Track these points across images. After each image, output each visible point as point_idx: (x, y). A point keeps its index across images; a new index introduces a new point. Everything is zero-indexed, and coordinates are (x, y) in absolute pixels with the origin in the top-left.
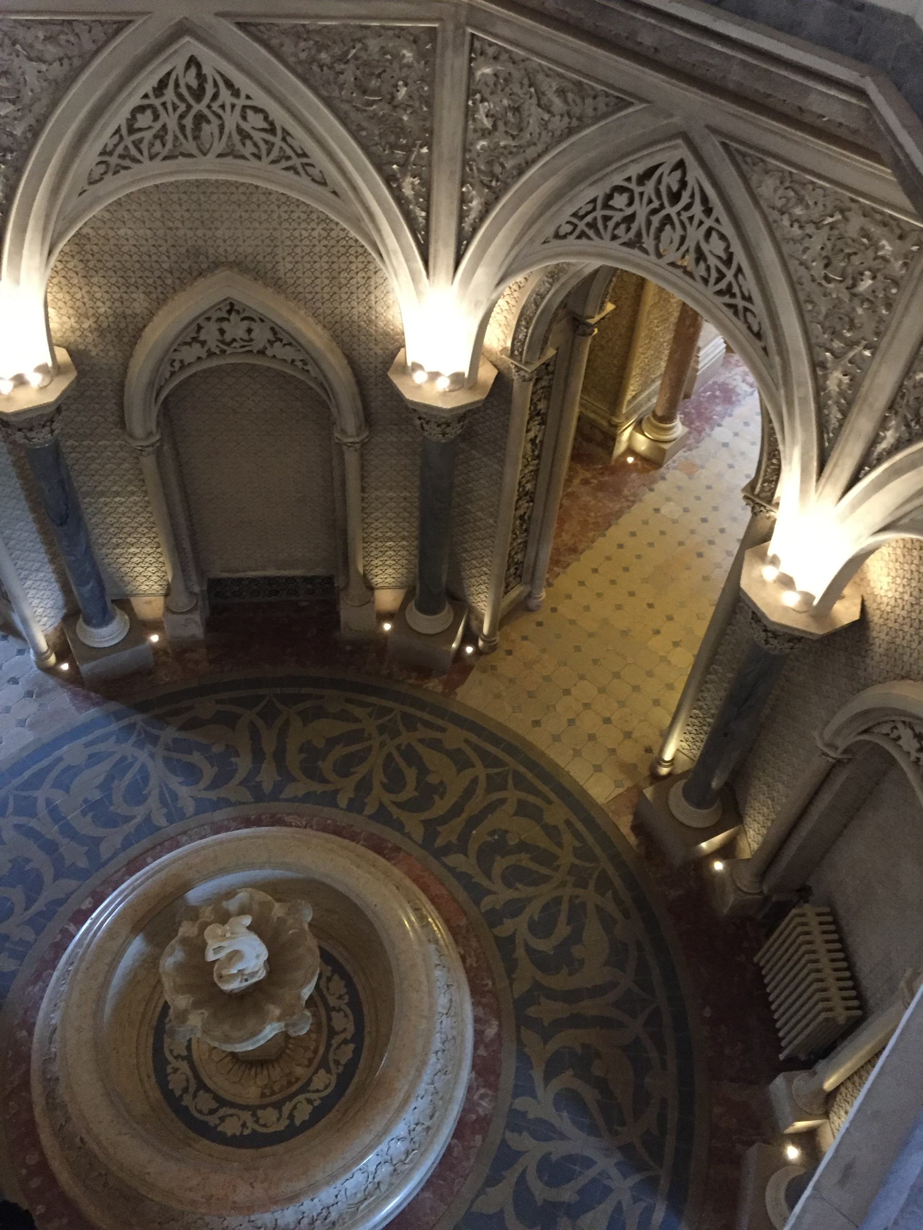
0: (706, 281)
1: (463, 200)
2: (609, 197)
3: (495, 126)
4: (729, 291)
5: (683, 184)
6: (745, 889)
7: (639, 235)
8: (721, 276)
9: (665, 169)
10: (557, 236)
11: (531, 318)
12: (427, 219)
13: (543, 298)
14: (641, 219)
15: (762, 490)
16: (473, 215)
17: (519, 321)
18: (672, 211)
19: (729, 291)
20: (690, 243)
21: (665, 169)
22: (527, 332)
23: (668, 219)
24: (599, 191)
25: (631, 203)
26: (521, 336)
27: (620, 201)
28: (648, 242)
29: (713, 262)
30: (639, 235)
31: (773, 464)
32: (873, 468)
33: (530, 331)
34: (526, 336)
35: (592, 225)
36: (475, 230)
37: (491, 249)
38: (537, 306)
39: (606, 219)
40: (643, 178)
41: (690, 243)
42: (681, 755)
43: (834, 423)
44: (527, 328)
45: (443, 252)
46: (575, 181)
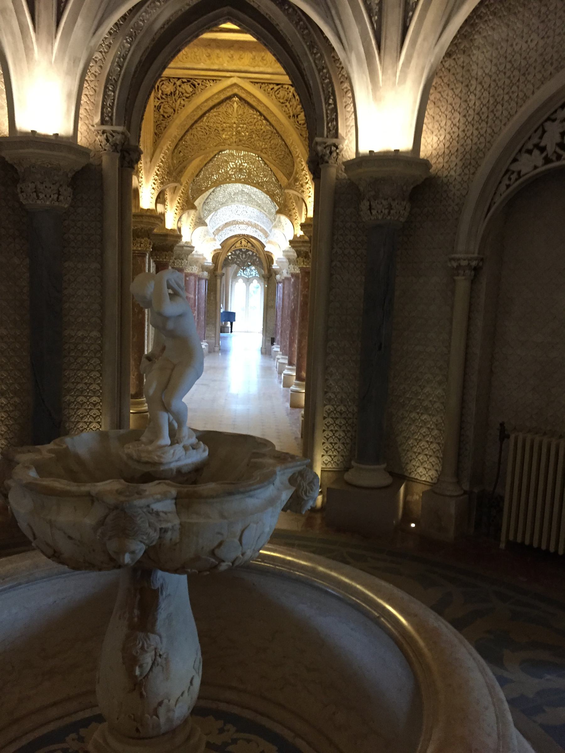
6: (456, 494)
11: (116, 82)
13: (124, 59)
15: (329, 130)
17: (106, 87)
22: (114, 96)
26: (109, 103)
31: (330, 104)
32: (414, 11)
33: (117, 92)
34: (114, 100)
37: (79, 21)
38: (121, 67)
42: (326, 474)
43: (376, 9)
44: (114, 92)
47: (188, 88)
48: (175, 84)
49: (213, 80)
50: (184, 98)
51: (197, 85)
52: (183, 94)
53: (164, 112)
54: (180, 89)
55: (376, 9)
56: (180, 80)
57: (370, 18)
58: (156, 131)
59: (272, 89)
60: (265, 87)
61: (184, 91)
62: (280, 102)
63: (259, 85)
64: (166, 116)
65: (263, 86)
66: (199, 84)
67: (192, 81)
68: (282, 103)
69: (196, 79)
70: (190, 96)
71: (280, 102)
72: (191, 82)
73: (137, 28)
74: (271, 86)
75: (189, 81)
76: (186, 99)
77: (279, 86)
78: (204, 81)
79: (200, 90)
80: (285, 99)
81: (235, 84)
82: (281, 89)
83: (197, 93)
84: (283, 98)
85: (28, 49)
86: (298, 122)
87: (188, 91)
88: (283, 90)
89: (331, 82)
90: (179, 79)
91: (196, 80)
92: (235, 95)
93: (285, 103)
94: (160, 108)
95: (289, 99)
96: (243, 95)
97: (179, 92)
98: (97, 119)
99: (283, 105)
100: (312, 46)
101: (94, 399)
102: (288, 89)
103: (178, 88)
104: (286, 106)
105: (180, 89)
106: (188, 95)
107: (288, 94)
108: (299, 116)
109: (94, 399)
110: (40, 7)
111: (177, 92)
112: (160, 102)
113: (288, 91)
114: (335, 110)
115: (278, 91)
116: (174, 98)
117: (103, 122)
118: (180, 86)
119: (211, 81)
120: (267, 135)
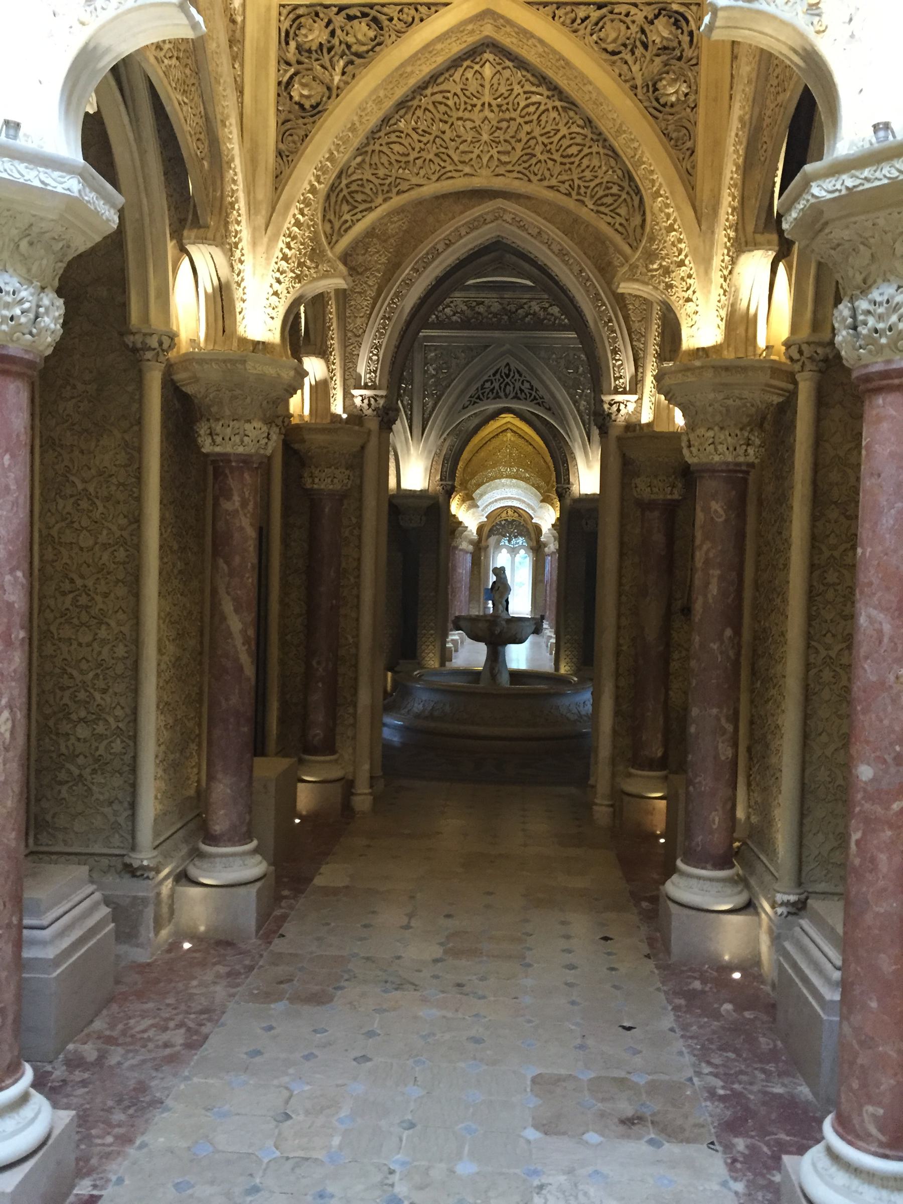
0: (526, 399)
1: (424, 405)
2: (484, 384)
3: (437, 373)
4: (535, 399)
5: (510, 370)
7: (497, 393)
8: (531, 394)
9: (503, 368)
10: (464, 408)
12: (411, 414)
14: (497, 387)
16: (428, 412)
18: (507, 380)
19: (535, 399)
20: (517, 388)
21: (503, 368)
23: (507, 384)
24: (479, 385)
25: (492, 383)
27: (488, 385)
28: (502, 394)
29: (527, 391)
30: (497, 393)
35: (478, 398)
36: (430, 415)
39: (483, 394)
40: (494, 375)
41: (517, 388)
45: (417, 430)
46: (468, 385)
55: (587, 421)
57: (584, 426)
73: (460, 431)
85: (408, 449)
89: (565, 456)
98: (438, 477)
100: (554, 436)
101: (432, 632)
109: (432, 632)
110: (414, 427)
114: (568, 470)
117: (441, 480)
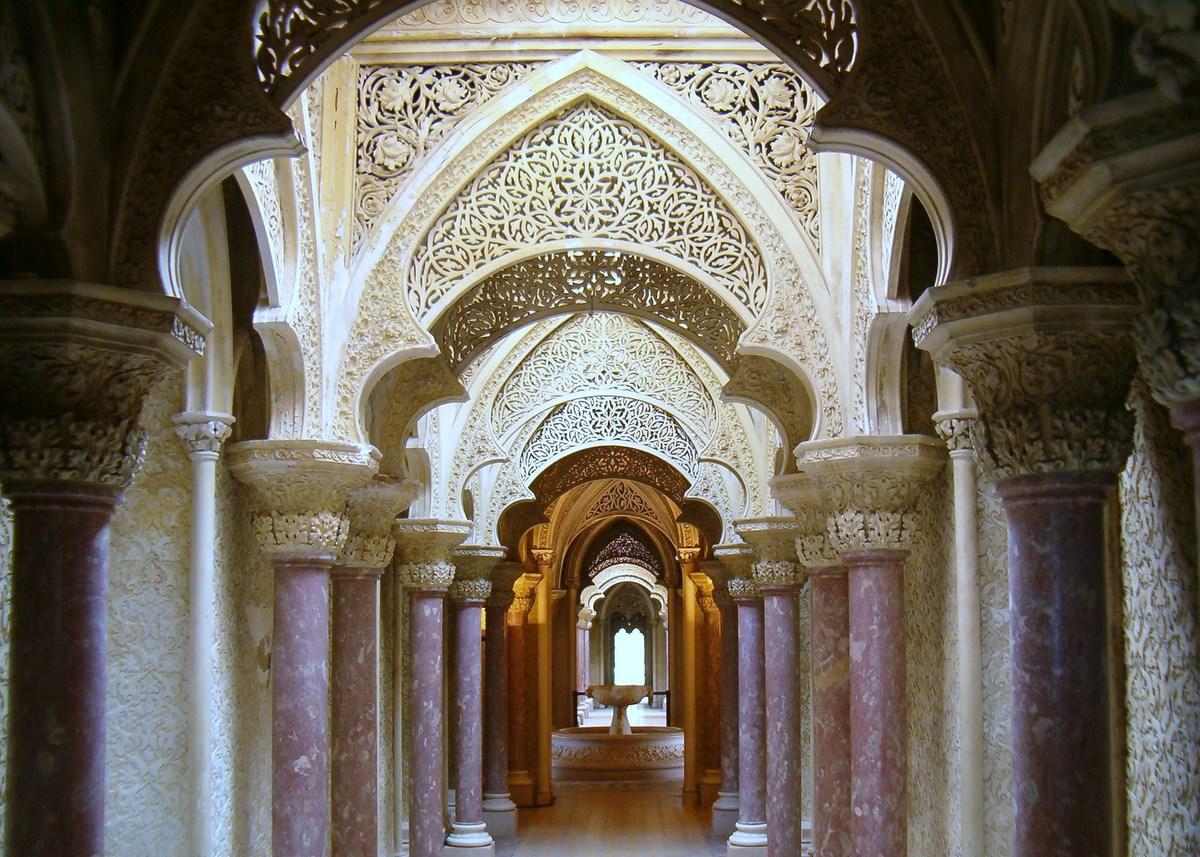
47: (450, 90)
48: (414, 81)
49: (525, 64)
50: (441, 115)
51: (477, 81)
52: (437, 105)
53: (385, 155)
54: (429, 93)
56: (432, 71)
58: (361, 211)
59: (688, 78)
60: (670, 72)
61: (439, 98)
62: (712, 108)
63: (654, 67)
64: (392, 167)
65: (664, 70)
66: (483, 78)
67: (464, 71)
68: (722, 112)
69: (475, 64)
70: (457, 110)
71: (712, 108)
72: (462, 74)
74: (685, 71)
75: (455, 73)
76: (446, 118)
77: (709, 69)
78: (500, 68)
79: (485, 92)
80: (728, 101)
81: (586, 72)
82: (716, 75)
83: (480, 100)
84: (722, 100)
86: (771, 160)
87: (451, 95)
88: (719, 79)
90: (426, 68)
91: (477, 68)
92: (586, 102)
93: (728, 111)
94: (375, 147)
95: (740, 100)
96: (609, 99)
97: (428, 100)
99: (725, 116)
102: (734, 74)
103: (425, 91)
104: (734, 121)
105: (429, 93)
106: (450, 107)
107: (735, 87)
108: (772, 144)
111: (422, 101)
112: (374, 131)
113: (735, 79)
115: (706, 83)
116: (412, 116)
118: (429, 87)
119: (518, 68)
120: (679, 206)
